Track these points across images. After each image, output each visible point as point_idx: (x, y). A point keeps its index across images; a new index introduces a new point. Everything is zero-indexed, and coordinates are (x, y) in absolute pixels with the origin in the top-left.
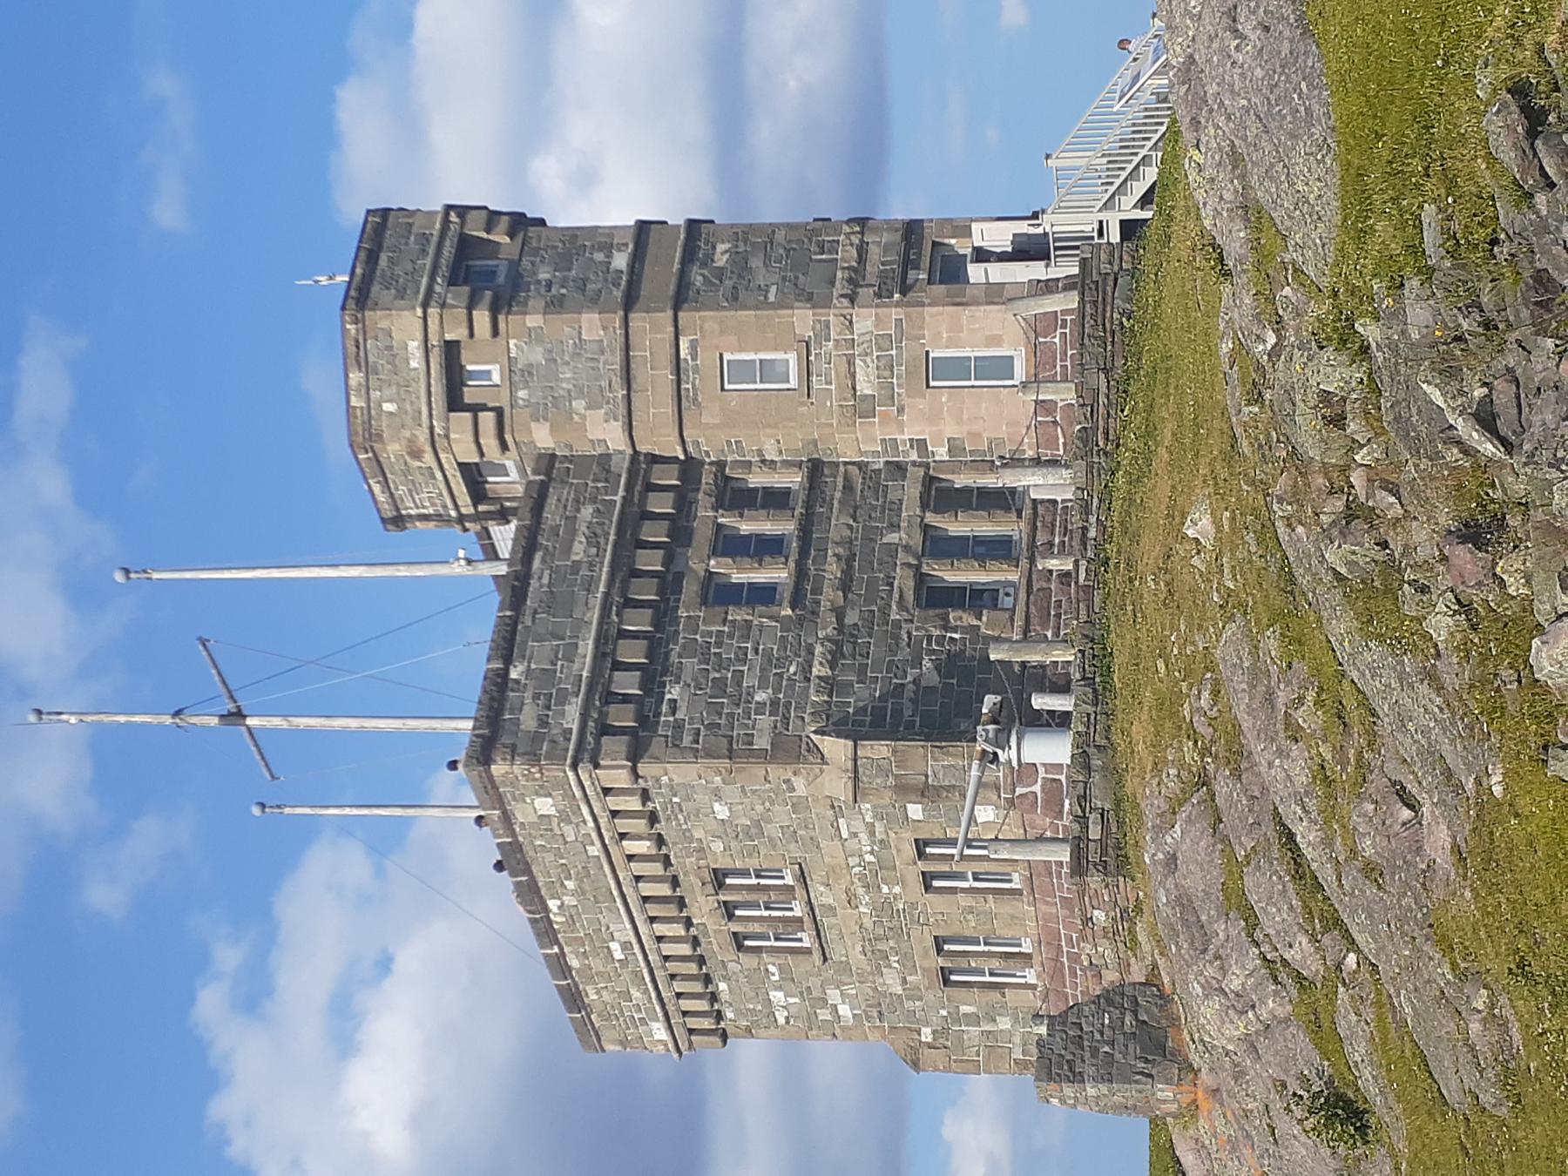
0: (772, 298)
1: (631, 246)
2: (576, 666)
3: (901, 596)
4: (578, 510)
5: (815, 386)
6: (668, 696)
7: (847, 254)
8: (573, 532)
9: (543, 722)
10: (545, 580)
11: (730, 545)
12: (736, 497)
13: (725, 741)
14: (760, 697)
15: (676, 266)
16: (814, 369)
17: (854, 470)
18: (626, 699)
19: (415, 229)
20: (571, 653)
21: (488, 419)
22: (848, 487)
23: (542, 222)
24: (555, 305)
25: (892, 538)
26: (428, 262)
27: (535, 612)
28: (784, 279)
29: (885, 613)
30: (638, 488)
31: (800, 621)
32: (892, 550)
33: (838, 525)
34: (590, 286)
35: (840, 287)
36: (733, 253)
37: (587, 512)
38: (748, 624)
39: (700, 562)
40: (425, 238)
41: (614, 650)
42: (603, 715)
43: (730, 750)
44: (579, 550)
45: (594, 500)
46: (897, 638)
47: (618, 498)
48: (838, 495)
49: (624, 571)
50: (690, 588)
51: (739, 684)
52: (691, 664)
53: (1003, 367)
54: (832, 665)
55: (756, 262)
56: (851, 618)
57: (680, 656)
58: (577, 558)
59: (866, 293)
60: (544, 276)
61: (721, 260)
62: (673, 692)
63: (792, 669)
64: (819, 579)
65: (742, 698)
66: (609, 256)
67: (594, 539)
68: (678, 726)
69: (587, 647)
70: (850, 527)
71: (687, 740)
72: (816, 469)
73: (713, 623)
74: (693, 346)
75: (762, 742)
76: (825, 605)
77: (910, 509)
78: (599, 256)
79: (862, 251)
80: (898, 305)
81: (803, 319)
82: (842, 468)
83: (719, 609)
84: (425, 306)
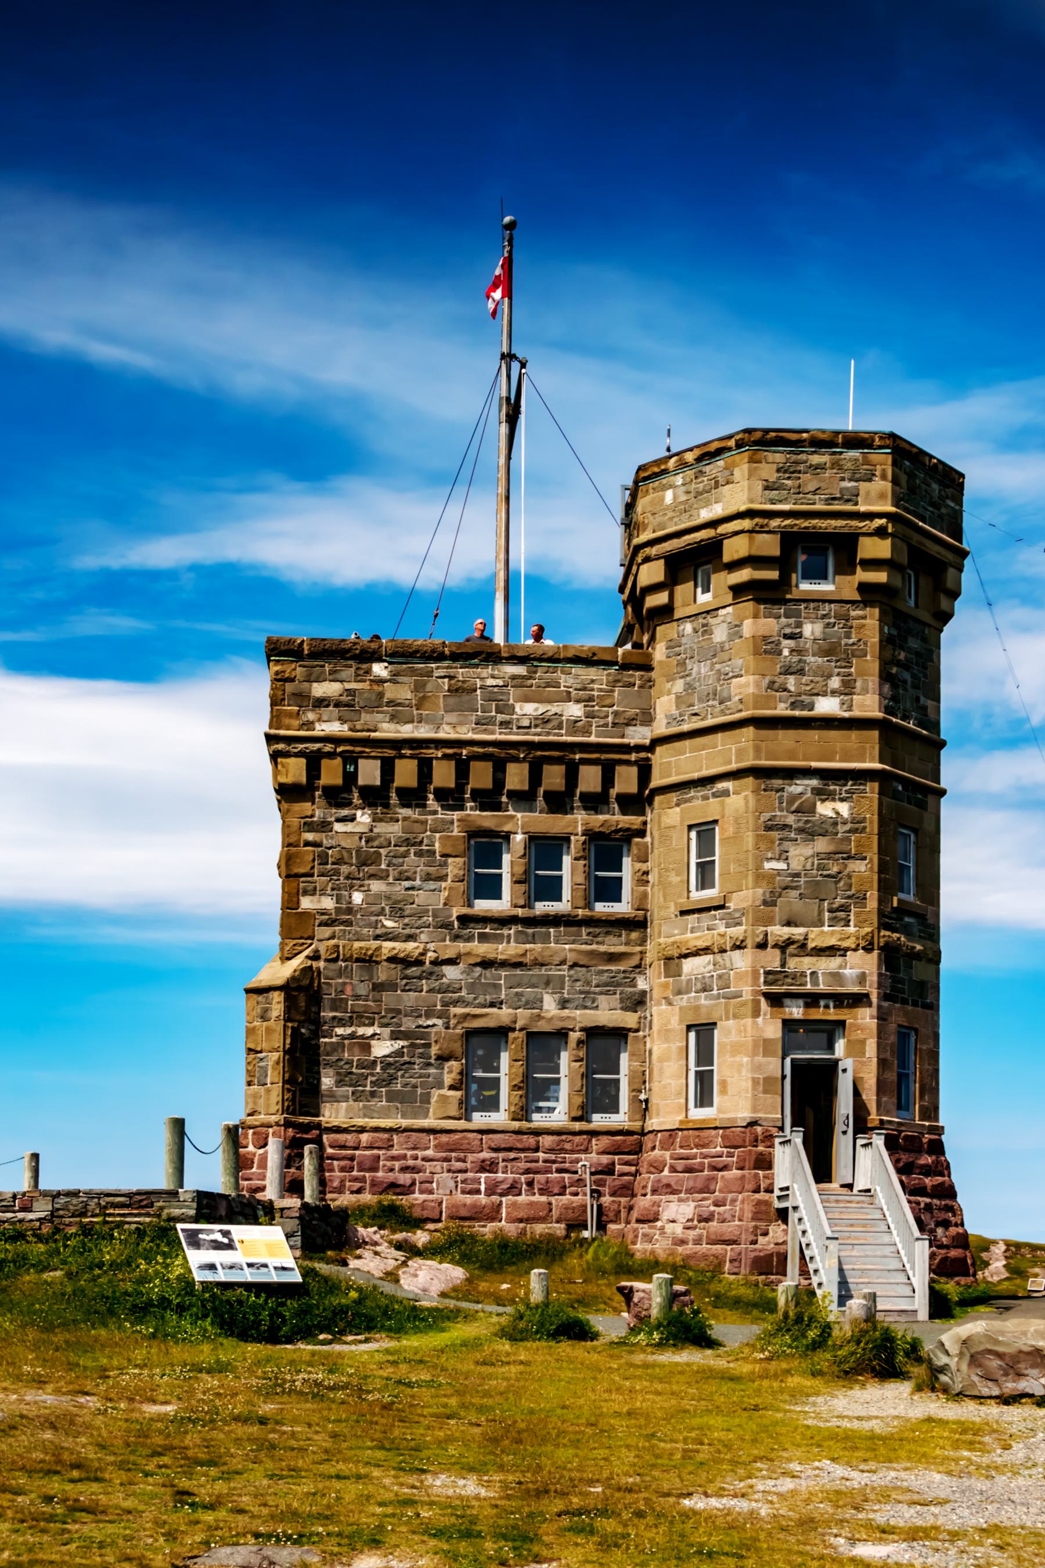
0: (768, 865)
1: (846, 715)
3: (475, 1016)
4: (578, 701)
6: (359, 813)
8: (550, 701)
10: (490, 682)
11: (546, 849)
12: (606, 850)
14: (357, 898)
16: (704, 915)
17: (635, 961)
22: (612, 958)
25: (549, 1004)
27: (451, 677)
29: (456, 1003)
30: (604, 756)
31: (448, 926)
35: (779, 932)
37: (575, 710)
38: (443, 878)
39: (520, 824)
41: (403, 757)
43: (298, 876)
44: (530, 709)
47: (593, 739)
48: (602, 948)
49: (499, 756)
50: (486, 819)
51: (372, 876)
52: (392, 830)
53: (704, 1098)
54: (393, 959)
56: (451, 973)
57: (405, 819)
58: (517, 709)
59: (772, 959)
62: (364, 818)
63: (389, 924)
64: (498, 939)
67: (544, 721)
70: (563, 962)
72: (637, 924)
73: (442, 845)
74: (726, 793)
76: (462, 946)
79: (831, 951)
80: (755, 993)
81: (746, 897)
82: (639, 949)
83: (461, 847)
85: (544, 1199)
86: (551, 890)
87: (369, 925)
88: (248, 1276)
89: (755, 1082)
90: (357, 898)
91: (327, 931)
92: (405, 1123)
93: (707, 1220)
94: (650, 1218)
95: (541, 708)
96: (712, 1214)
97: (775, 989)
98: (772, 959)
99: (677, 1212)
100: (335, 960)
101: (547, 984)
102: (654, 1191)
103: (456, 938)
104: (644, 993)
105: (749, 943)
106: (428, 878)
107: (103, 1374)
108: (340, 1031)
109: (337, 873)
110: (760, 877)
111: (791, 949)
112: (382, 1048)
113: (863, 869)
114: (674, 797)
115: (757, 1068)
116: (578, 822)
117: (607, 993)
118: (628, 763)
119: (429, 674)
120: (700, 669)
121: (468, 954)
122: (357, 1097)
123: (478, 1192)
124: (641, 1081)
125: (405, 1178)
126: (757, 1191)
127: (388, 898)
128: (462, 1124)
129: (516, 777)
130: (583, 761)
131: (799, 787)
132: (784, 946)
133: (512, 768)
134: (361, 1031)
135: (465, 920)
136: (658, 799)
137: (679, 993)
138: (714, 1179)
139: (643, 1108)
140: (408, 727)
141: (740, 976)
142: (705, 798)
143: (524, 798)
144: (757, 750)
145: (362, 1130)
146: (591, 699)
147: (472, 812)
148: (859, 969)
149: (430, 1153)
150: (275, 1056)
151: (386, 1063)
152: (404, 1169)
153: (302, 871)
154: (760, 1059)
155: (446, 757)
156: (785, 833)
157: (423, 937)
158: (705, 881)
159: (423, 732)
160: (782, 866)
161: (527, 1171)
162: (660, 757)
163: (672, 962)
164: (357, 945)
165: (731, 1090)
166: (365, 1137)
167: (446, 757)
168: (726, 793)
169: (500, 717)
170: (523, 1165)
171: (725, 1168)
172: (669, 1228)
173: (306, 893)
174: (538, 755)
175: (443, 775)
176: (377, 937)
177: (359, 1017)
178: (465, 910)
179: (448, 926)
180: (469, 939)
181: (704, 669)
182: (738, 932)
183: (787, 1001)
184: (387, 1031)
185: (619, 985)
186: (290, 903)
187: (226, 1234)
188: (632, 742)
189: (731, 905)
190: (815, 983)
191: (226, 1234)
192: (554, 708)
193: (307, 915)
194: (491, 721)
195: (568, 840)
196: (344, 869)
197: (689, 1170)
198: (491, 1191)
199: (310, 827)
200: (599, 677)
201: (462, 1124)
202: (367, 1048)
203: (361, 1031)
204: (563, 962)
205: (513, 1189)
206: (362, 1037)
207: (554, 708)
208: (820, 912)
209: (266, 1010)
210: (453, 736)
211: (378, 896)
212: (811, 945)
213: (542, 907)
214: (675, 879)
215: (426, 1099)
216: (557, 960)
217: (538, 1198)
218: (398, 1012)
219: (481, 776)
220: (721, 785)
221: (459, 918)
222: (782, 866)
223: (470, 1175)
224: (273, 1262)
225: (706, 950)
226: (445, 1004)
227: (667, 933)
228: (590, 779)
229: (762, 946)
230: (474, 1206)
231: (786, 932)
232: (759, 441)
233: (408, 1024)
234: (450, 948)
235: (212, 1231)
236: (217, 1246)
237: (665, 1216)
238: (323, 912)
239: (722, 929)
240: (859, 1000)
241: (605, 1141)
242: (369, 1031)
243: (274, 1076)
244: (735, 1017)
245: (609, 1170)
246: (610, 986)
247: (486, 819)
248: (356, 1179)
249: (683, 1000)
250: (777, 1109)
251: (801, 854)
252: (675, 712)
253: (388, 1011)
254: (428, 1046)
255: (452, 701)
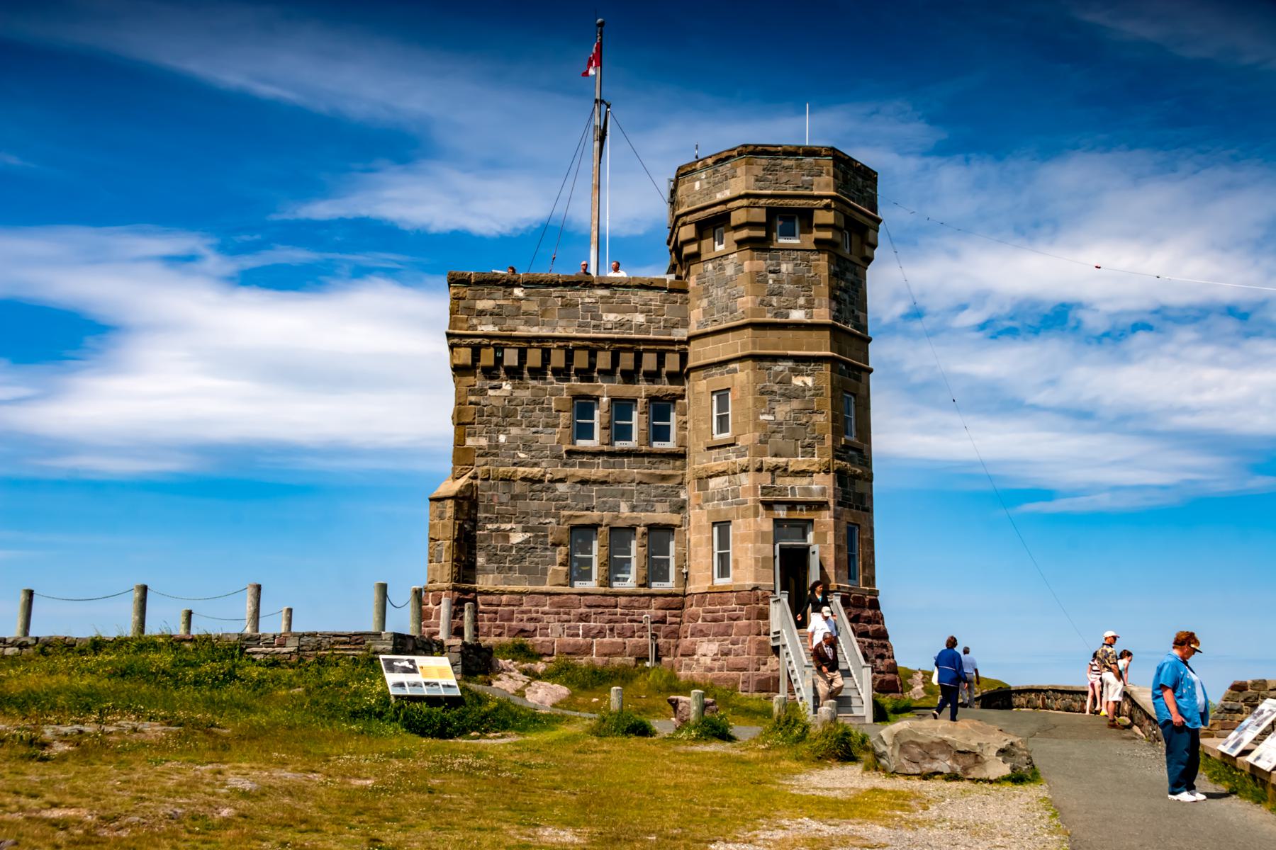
0: (762, 417)
2: (521, 327)
3: (577, 517)
4: (642, 312)
5: (714, 452)
7: (799, 463)
8: (624, 312)
9: (481, 313)
10: (587, 300)
11: (622, 407)
12: (660, 408)
13: (470, 420)
14: (502, 438)
15: (790, 352)
16: (722, 450)
17: (678, 480)
18: (499, 361)
19: (816, 179)
20: (527, 323)
21: (692, 248)
22: (664, 478)
23: (869, 260)
24: (758, 279)
25: (624, 509)
26: (789, 192)
28: (781, 424)
29: (564, 508)
30: (658, 347)
31: (559, 457)
32: (615, 508)
33: (632, 470)
34: (774, 300)
35: (770, 461)
36: (804, 389)
37: (640, 318)
38: (556, 426)
40: (810, 186)
41: (532, 347)
42: (487, 346)
44: (612, 317)
45: (649, 321)
46: (546, 516)
47: (651, 336)
48: (658, 472)
50: (584, 388)
51: (512, 424)
52: (525, 394)
53: (724, 572)
54: (524, 479)
55: (796, 404)
56: (561, 488)
59: (766, 479)
60: (784, 267)
61: (797, 381)
62: (507, 386)
63: (522, 455)
64: (592, 465)
65: (500, 428)
66: (801, 307)
67: (621, 325)
68: (482, 392)
69: (535, 331)
70: (633, 481)
71: (473, 398)
72: (680, 456)
73: (557, 404)
74: (735, 371)
75: (470, 442)
76: (569, 470)
77: (646, 517)
78: (802, 301)
80: (755, 501)
83: (569, 405)
84: (747, 196)
85: (620, 640)
86: (625, 433)
87: (509, 456)
88: (425, 691)
89: (756, 560)
90: (502, 438)
91: (483, 460)
92: (531, 588)
93: (727, 654)
94: (690, 654)
95: (619, 317)
96: (730, 650)
97: (768, 498)
98: (766, 479)
99: (707, 649)
100: (487, 479)
101: (623, 495)
102: (692, 635)
103: (565, 465)
104: (684, 501)
105: (751, 468)
106: (547, 425)
107: (326, 758)
108: (489, 526)
109: (490, 422)
110: (758, 425)
111: (778, 472)
112: (517, 538)
113: (822, 420)
114: (702, 373)
115: (758, 551)
116: (642, 389)
117: (661, 501)
118: (673, 351)
119: (549, 295)
120: (718, 292)
121: (573, 475)
122: (500, 570)
123: (578, 635)
124: (683, 560)
125: (530, 626)
126: (759, 634)
127: (521, 438)
128: (567, 589)
129: (603, 361)
130: (645, 351)
131: (781, 367)
132: (774, 470)
133: (600, 355)
134: (503, 526)
135: (569, 453)
136: (692, 375)
137: (707, 501)
138: (731, 626)
139: (685, 578)
140: (536, 328)
141: (746, 490)
142: (722, 374)
143: (608, 374)
144: (754, 343)
145: (503, 593)
146: (650, 311)
147: (575, 384)
148: (822, 485)
149: (546, 608)
150: (448, 543)
151: (519, 547)
152: (530, 620)
153: (467, 421)
154: (759, 545)
155: (559, 347)
156: (772, 397)
157: (544, 464)
158: (723, 426)
159: (545, 332)
160: (771, 418)
161: (610, 621)
162: (693, 348)
163: (702, 480)
164: (501, 469)
165: (741, 566)
166: (504, 598)
167: (559, 347)
168: (735, 371)
169: (593, 322)
170: (607, 617)
171: (738, 619)
172: (702, 659)
173: (469, 435)
174: (618, 347)
175: (558, 359)
176: (514, 464)
177: (501, 518)
178: (571, 447)
179: (559, 457)
180: (573, 466)
181: (720, 292)
182: (744, 461)
183: (776, 506)
184: (520, 526)
185: (668, 496)
186: (459, 443)
187: (412, 662)
188: (676, 338)
189: (739, 443)
190: (794, 494)
191: (412, 662)
192: (627, 317)
193: (469, 449)
194: (588, 325)
195: (635, 401)
196: (494, 420)
197: (715, 620)
198: (586, 635)
199: (473, 392)
200: (654, 297)
201: (567, 589)
202: (507, 538)
203: (503, 526)
204: (633, 481)
205: (601, 633)
206: (504, 530)
207: (627, 317)
208: (796, 448)
209: (442, 512)
210: (564, 334)
211: (516, 437)
212: (790, 469)
213: (620, 445)
214: (703, 426)
215: (545, 572)
216: (629, 479)
217: (617, 639)
218: (527, 513)
219: (581, 360)
220: (732, 366)
221: (567, 452)
222: (771, 418)
223: (572, 624)
224: (442, 681)
225: (724, 473)
226: (557, 509)
227: (699, 461)
228: (649, 362)
229: (759, 470)
230: (575, 645)
231: (774, 461)
232: (752, 152)
233: (534, 522)
234: (561, 472)
235: (402, 660)
236: (406, 670)
237: (700, 652)
238: (480, 448)
239: (734, 459)
240: (821, 505)
241: (661, 600)
242: (508, 526)
243: (446, 556)
244: (743, 517)
245: (663, 621)
246: (663, 497)
247: (584, 388)
248: (498, 627)
249: (710, 506)
250: (771, 579)
251: (783, 410)
252: (702, 319)
253: (521, 513)
254: (546, 536)
255: (563, 312)
